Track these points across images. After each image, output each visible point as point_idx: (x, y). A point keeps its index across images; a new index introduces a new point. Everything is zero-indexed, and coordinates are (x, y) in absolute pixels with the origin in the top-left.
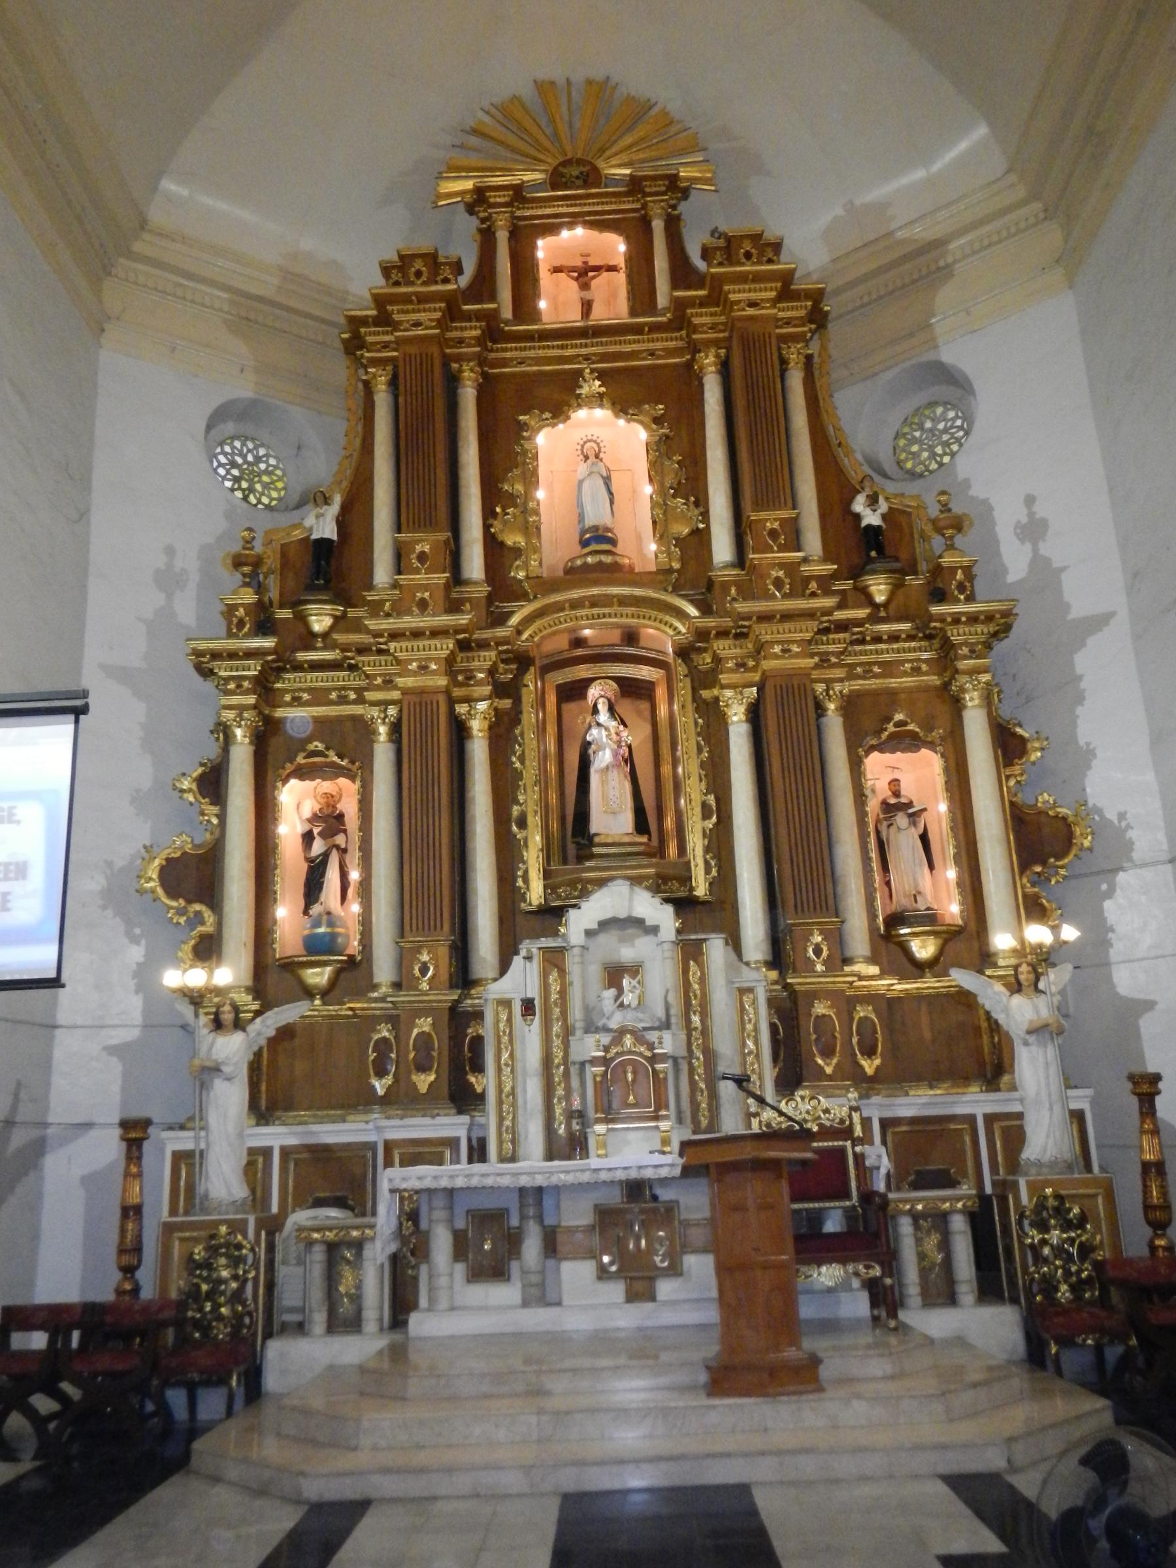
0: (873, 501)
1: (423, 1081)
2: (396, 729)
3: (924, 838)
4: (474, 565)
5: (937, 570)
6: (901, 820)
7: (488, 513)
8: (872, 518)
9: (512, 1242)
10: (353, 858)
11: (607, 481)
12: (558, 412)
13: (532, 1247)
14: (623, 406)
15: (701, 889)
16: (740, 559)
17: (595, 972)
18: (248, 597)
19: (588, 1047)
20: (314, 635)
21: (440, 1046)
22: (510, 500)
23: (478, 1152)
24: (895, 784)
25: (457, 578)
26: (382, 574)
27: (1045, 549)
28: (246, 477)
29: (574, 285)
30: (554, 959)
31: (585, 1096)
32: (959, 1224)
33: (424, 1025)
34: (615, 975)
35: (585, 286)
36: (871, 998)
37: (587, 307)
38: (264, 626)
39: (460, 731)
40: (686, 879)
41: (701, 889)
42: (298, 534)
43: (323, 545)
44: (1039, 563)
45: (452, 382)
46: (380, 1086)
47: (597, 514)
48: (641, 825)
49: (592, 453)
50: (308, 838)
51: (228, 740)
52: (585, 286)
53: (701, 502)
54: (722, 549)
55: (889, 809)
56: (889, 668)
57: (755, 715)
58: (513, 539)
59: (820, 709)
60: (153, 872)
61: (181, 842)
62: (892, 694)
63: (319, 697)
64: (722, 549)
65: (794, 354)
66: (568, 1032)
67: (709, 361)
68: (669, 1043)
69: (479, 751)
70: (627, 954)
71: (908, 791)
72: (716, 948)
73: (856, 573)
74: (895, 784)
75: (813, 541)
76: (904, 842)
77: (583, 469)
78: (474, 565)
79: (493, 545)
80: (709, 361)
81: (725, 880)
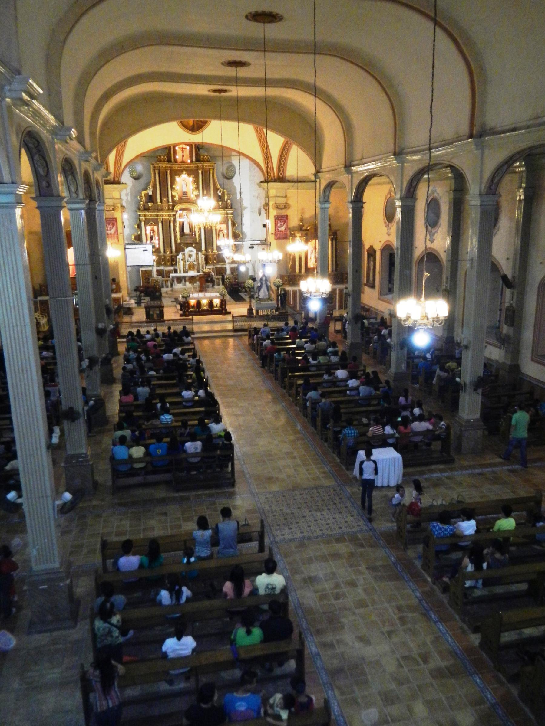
0: (220, 192)
1: (169, 263)
2: (162, 222)
4: (170, 200)
5: (227, 204)
6: (221, 232)
7: (171, 191)
8: (220, 194)
12: (179, 175)
13: (183, 281)
14: (189, 175)
15: (198, 241)
19: (187, 263)
20: (149, 207)
21: (170, 259)
22: (174, 189)
23: (176, 271)
25: (168, 202)
26: (159, 200)
30: (184, 254)
31: (187, 268)
32: (220, 279)
33: (168, 258)
35: (183, 152)
36: (215, 254)
37: (183, 156)
39: (170, 222)
41: (198, 241)
45: (167, 172)
46: (163, 263)
47: (185, 190)
48: (190, 231)
49: (184, 180)
51: (141, 222)
52: (183, 152)
55: (220, 231)
58: (174, 194)
60: (133, 237)
63: (151, 215)
65: (211, 172)
66: (185, 262)
67: (200, 172)
68: (195, 263)
69: (172, 224)
70: (191, 253)
71: (222, 229)
72: (200, 253)
78: (170, 200)
79: (172, 195)
80: (200, 172)
81: (200, 240)
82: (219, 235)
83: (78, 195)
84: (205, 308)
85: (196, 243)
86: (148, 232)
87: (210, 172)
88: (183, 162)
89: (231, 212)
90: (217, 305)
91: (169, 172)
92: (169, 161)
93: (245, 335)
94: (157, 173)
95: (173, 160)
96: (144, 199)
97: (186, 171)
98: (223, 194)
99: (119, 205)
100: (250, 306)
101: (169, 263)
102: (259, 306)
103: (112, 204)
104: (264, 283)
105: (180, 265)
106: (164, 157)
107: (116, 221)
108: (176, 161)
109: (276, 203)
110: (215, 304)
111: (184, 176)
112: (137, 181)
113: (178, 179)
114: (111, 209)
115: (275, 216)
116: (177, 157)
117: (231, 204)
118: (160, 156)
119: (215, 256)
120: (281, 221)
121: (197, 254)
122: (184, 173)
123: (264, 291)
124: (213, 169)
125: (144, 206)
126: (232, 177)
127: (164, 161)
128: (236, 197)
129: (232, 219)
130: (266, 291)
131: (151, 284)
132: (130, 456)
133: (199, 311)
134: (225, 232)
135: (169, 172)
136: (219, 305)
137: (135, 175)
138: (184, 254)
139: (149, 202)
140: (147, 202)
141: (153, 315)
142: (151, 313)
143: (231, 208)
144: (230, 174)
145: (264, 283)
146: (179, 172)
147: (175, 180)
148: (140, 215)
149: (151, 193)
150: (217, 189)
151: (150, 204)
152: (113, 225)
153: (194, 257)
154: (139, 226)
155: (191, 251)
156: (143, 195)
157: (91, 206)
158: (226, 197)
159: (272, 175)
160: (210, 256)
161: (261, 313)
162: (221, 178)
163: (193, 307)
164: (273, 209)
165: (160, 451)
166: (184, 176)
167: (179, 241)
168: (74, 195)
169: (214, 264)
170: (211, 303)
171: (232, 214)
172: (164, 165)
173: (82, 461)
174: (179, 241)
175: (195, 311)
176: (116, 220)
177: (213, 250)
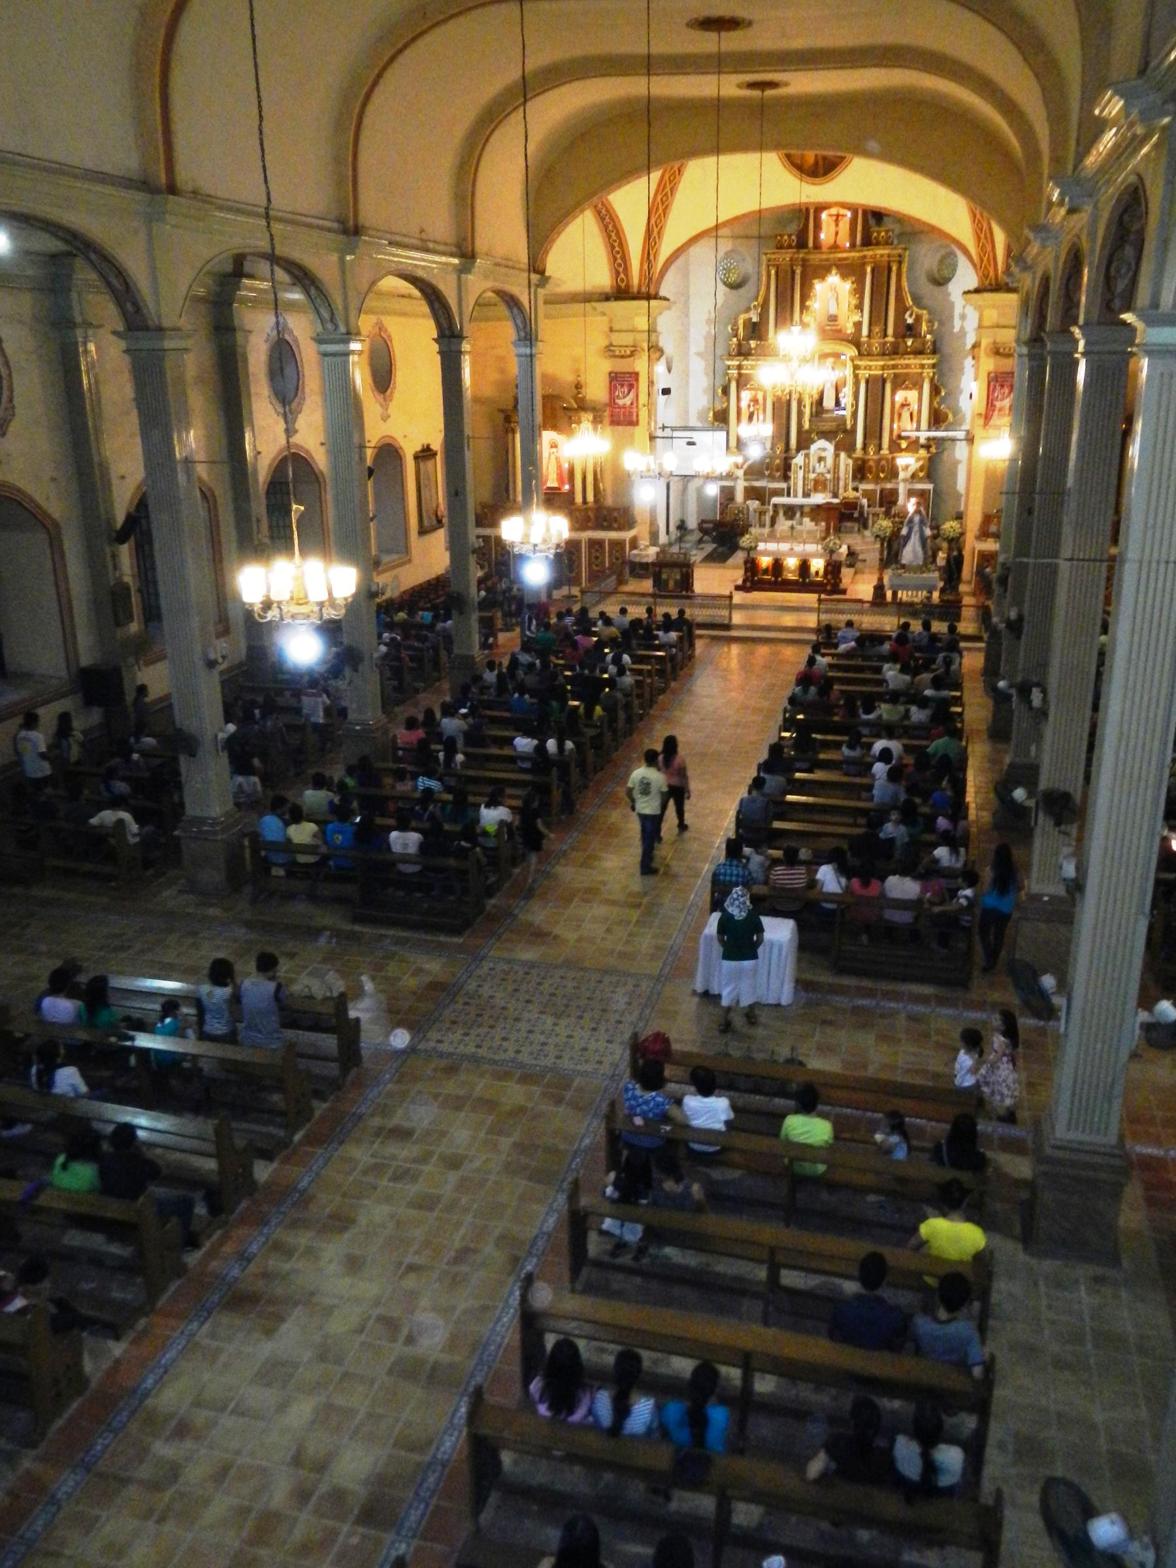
0: (911, 315)
1: (778, 474)
3: (911, 415)
5: (924, 343)
6: (906, 408)
8: (910, 321)
9: (794, 515)
10: (761, 412)
11: (837, 299)
12: (823, 278)
13: (798, 515)
14: (844, 276)
15: (849, 427)
16: (869, 336)
17: (816, 459)
18: (735, 340)
19: (812, 476)
21: (782, 466)
22: (807, 308)
24: (906, 399)
27: (965, 324)
28: (728, 270)
29: (833, 224)
30: (807, 456)
31: (811, 486)
33: (778, 461)
34: (821, 459)
35: (837, 225)
37: (837, 233)
38: (739, 354)
40: (845, 424)
41: (849, 427)
42: (746, 316)
43: (755, 324)
44: (962, 327)
45: (793, 272)
46: (767, 473)
49: (834, 289)
50: (749, 406)
52: (837, 225)
53: (862, 311)
54: (865, 332)
55: (903, 406)
56: (908, 366)
57: (867, 382)
59: (884, 381)
61: (718, 407)
62: (907, 374)
64: (865, 332)
65: (894, 268)
67: (869, 269)
68: (828, 476)
70: (823, 454)
71: (909, 400)
73: (904, 337)
74: (906, 399)
75: (890, 331)
76: (906, 415)
77: (830, 294)
81: (854, 425)
82: (900, 415)
83: (336, 327)
84: (791, 577)
85: (845, 431)
86: (744, 404)
87: (890, 270)
88: (835, 247)
89: (931, 362)
90: (817, 573)
91: (798, 271)
92: (802, 244)
93: (979, 649)
94: (773, 272)
95: (811, 244)
96: (741, 331)
97: (838, 267)
98: (918, 319)
99: (645, 345)
100: (881, 579)
101: (778, 474)
102: (897, 582)
103: (631, 343)
104: (916, 528)
105: (797, 477)
106: (790, 236)
107: (637, 380)
108: (817, 246)
109: (995, 343)
110: (813, 570)
111: (834, 279)
112: (734, 292)
113: (819, 287)
114: (628, 352)
115: (989, 374)
116: (822, 236)
117: (934, 343)
118: (781, 236)
119: (883, 462)
120: (1002, 386)
121: (837, 456)
122: (834, 271)
123: (914, 547)
124: (900, 263)
125: (739, 345)
126: (949, 279)
127: (790, 247)
128: (953, 327)
129: (932, 380)
130: (919, 549)
131: (728, 519)
132: (289, 841)
133: (776, 582)
134: (915, 407)
135: (798, 271)
136: (821, 572)
137: (733, 278)
138: (807, 456)
139: (752, 338)
140: (748, 338)
141: (667, 581)
142: (664, 576)
143: (934, 352)
144: (946, 273)
145: (916, 528)
146: (822, 271)
147: (811, 286)
148: (729, 367)
149: (755, 319)
150: (906, 309)
151: (753, 344)
152: (631, 387)
153: (830, 461)
154: (726, 391)
155: (824, 450)
156: (741, 322)
157: (453, 348)
158: (924, 328)
159: (992, 274)
160: (871, 463)
161: (903, 596)
162: (923, 280)
163: (766, 571)
164: (987, 355)
165: (340, 837)
166: (834, 279)
167: (807, 426)
168: (330, 326)
169: (877, 480)
170: (804, 567)
171: (934, 366)
172: (786, 256)
173: (207, 832)
174: (807, 426)
175: (768, 582)
176: (636, 375)
177: (880, 448)
